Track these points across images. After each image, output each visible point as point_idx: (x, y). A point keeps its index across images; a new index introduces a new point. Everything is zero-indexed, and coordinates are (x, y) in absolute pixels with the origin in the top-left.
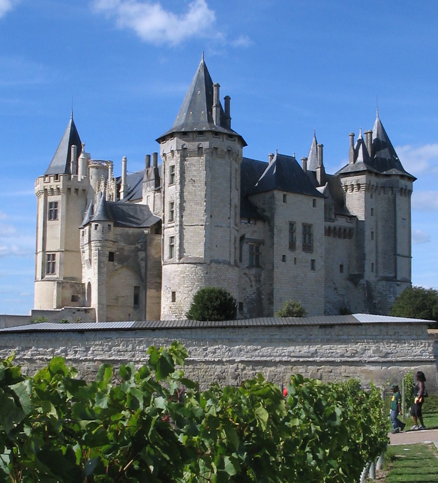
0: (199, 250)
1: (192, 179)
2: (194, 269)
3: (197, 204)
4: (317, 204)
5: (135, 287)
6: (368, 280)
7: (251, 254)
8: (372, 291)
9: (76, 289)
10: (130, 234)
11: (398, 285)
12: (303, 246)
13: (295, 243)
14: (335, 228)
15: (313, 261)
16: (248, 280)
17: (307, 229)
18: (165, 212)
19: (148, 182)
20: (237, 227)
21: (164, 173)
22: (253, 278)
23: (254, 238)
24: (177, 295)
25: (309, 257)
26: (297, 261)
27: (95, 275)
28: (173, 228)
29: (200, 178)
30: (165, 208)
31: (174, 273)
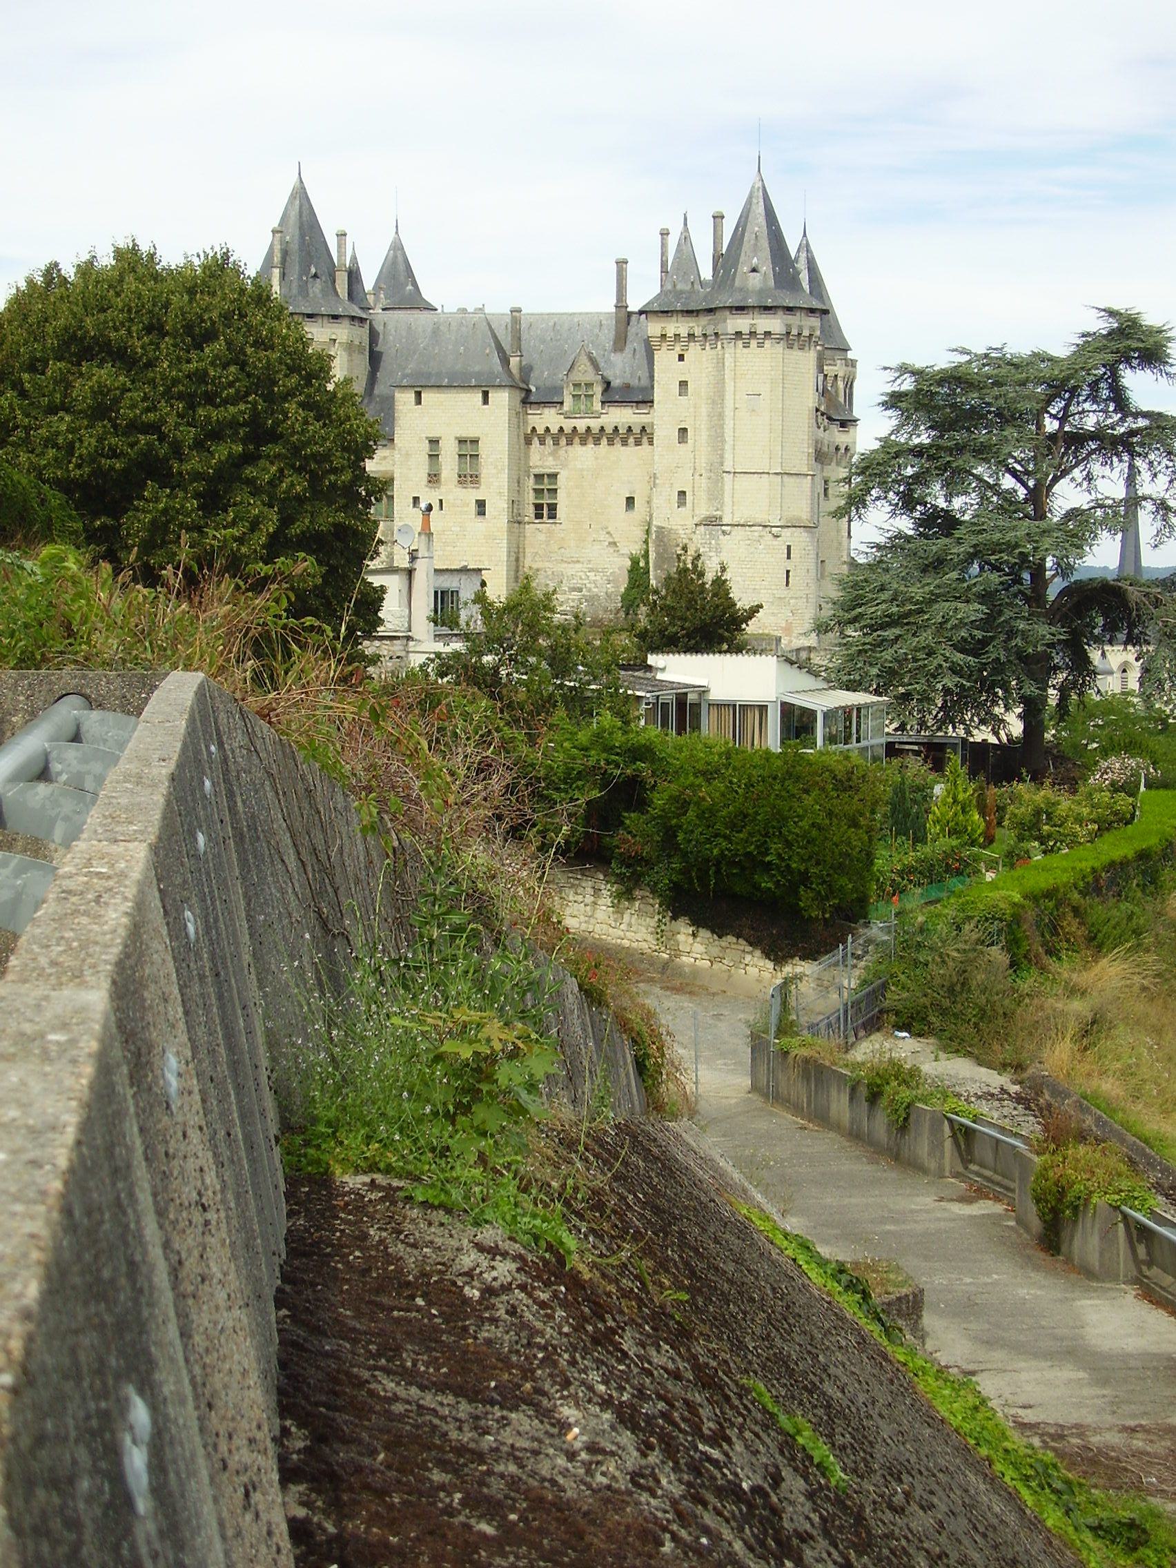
11: (724, 532)
14: (602, 429)
15: (481, 505)
17: (469, 448)
25: (472, 495)
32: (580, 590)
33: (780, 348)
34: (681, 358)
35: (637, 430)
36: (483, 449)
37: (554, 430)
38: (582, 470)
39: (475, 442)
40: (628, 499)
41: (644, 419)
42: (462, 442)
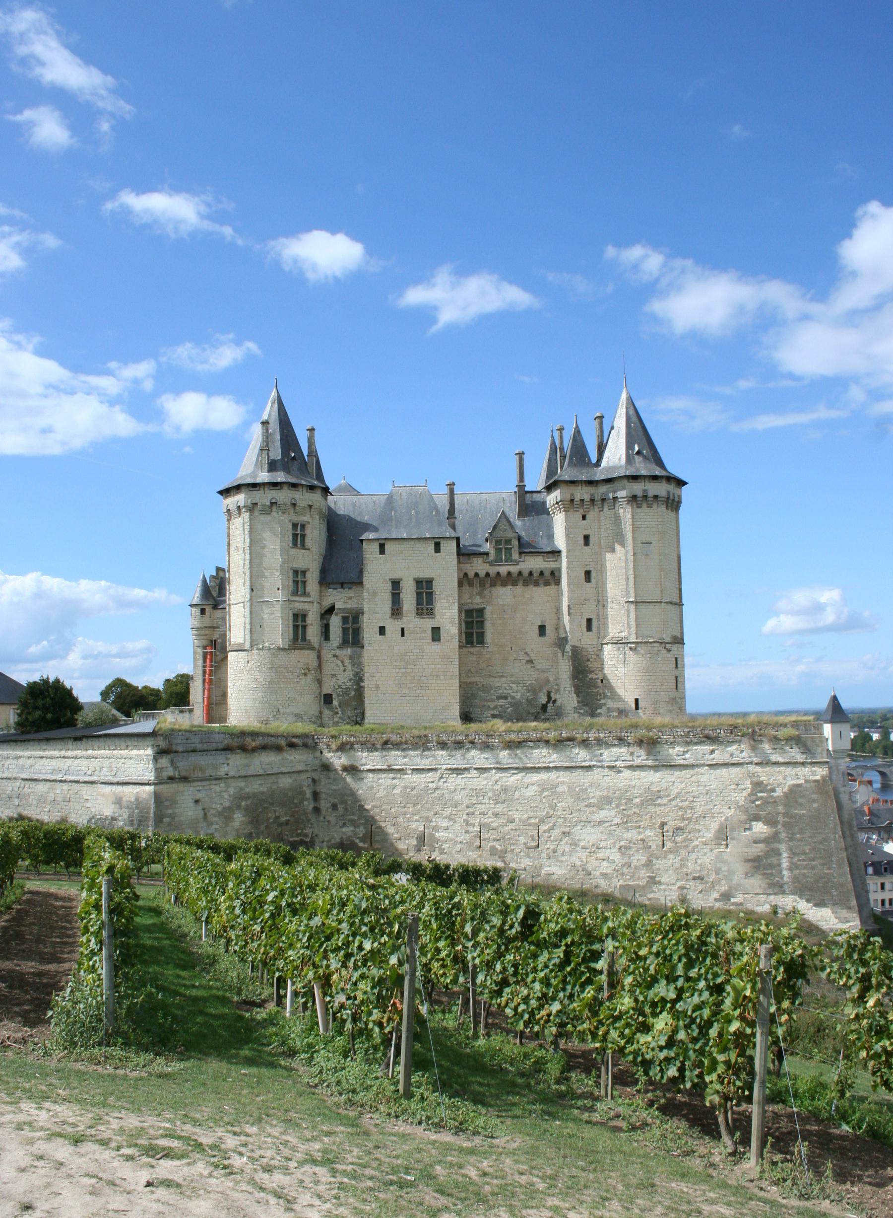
4: (442, 548)
6: (578, 644)
7: (345, 630)
8: (588, 660)
12: (418, 609)
13: (401, 608)
14: (520, 573)
16: (340, 663)
20: (309, 596)
22: (347, 662)
23: (348, 606)
25: (428, 624)
26: (406, 632)
32: (506, 698)
33: (663, 508)
34: (584, 518)
35: (547, 574)
36: (437, 587)
37: (482, 574)
38: (503, 605)
39: (429, 582)
40: (540, 627)
41: (553, 565)
42: (419, 582)
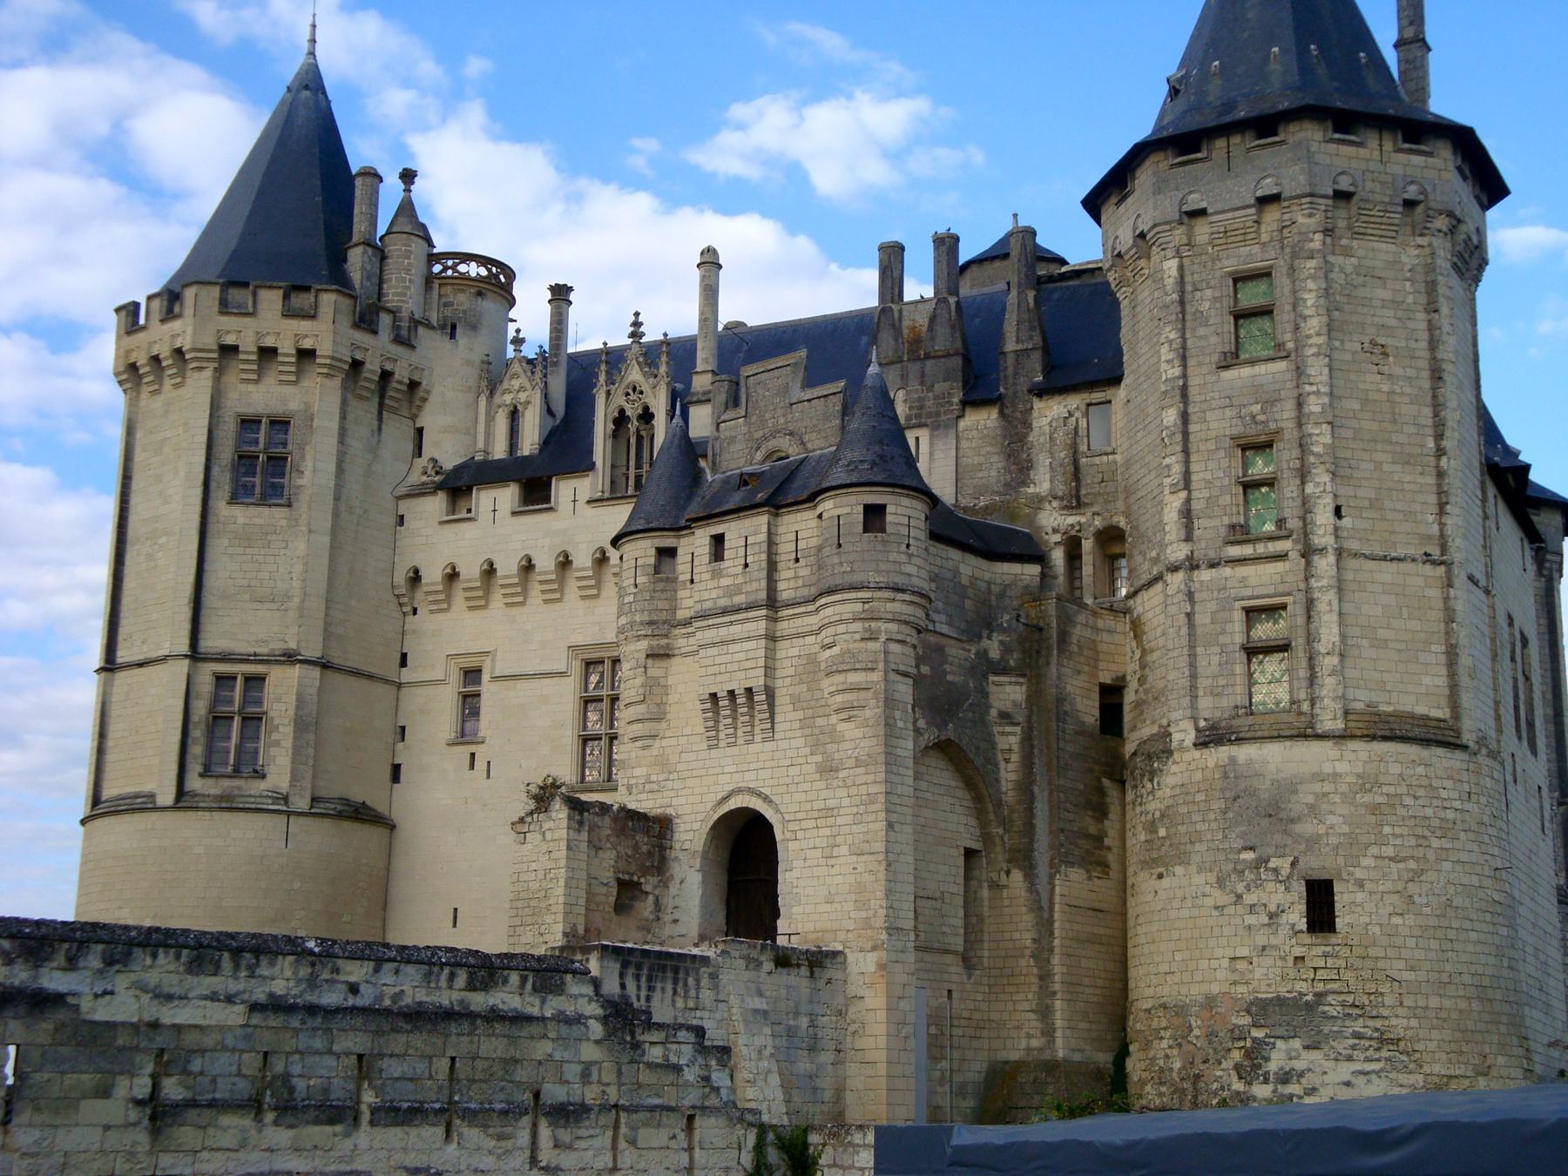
0: (1426, 680)
1: (1373, 343)
2: (1421, 770)
3: (1407, 461)
5: (969, 854)
9: (636, 847)
10: (965, 581)
18: (1194, 486)
19: (914, 368)
21: (1182, 303)
24: (1343, 897)
27: (828, 770)
28: (1279, 567)
29: (1413, 344)
30: (1194, 467)
31: (1317, 788)
